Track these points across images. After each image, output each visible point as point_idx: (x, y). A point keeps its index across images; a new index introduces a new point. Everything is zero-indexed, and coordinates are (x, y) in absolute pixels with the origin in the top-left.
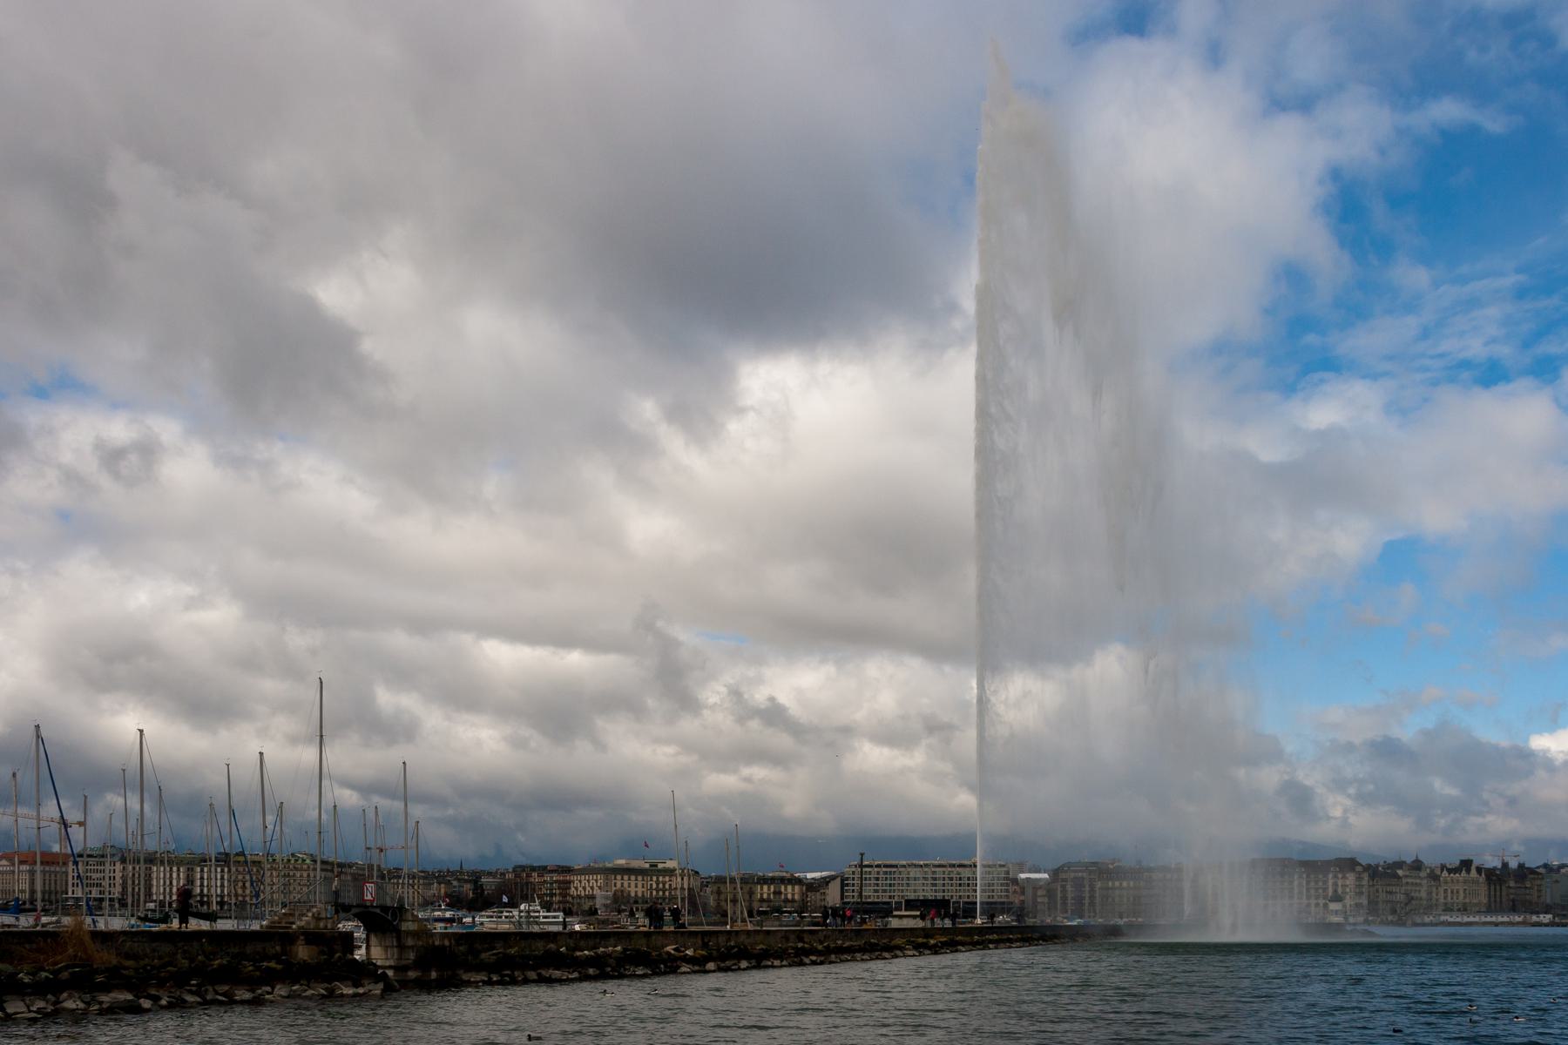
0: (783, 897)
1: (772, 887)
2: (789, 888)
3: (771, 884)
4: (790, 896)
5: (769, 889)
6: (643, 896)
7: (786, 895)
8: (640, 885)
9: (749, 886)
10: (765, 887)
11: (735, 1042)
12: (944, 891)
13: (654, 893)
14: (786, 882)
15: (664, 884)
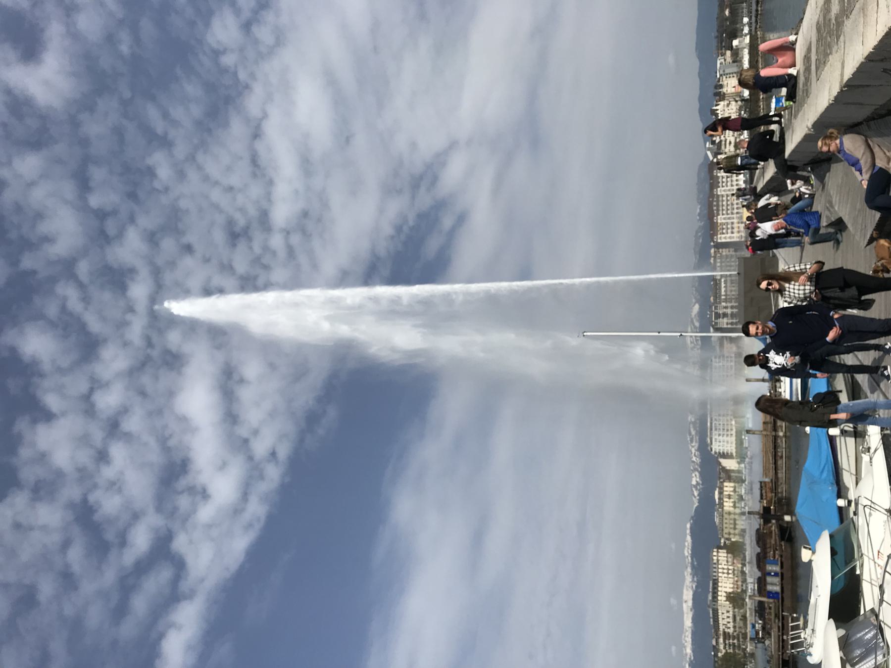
0: (732, 493)
1: (725, 500)
2: (725, 489)
4: (732, 489)
6: (733, 583)
7: (731, 491)
9: (724, 515)
10: (725, 504)
13: (731, 576)
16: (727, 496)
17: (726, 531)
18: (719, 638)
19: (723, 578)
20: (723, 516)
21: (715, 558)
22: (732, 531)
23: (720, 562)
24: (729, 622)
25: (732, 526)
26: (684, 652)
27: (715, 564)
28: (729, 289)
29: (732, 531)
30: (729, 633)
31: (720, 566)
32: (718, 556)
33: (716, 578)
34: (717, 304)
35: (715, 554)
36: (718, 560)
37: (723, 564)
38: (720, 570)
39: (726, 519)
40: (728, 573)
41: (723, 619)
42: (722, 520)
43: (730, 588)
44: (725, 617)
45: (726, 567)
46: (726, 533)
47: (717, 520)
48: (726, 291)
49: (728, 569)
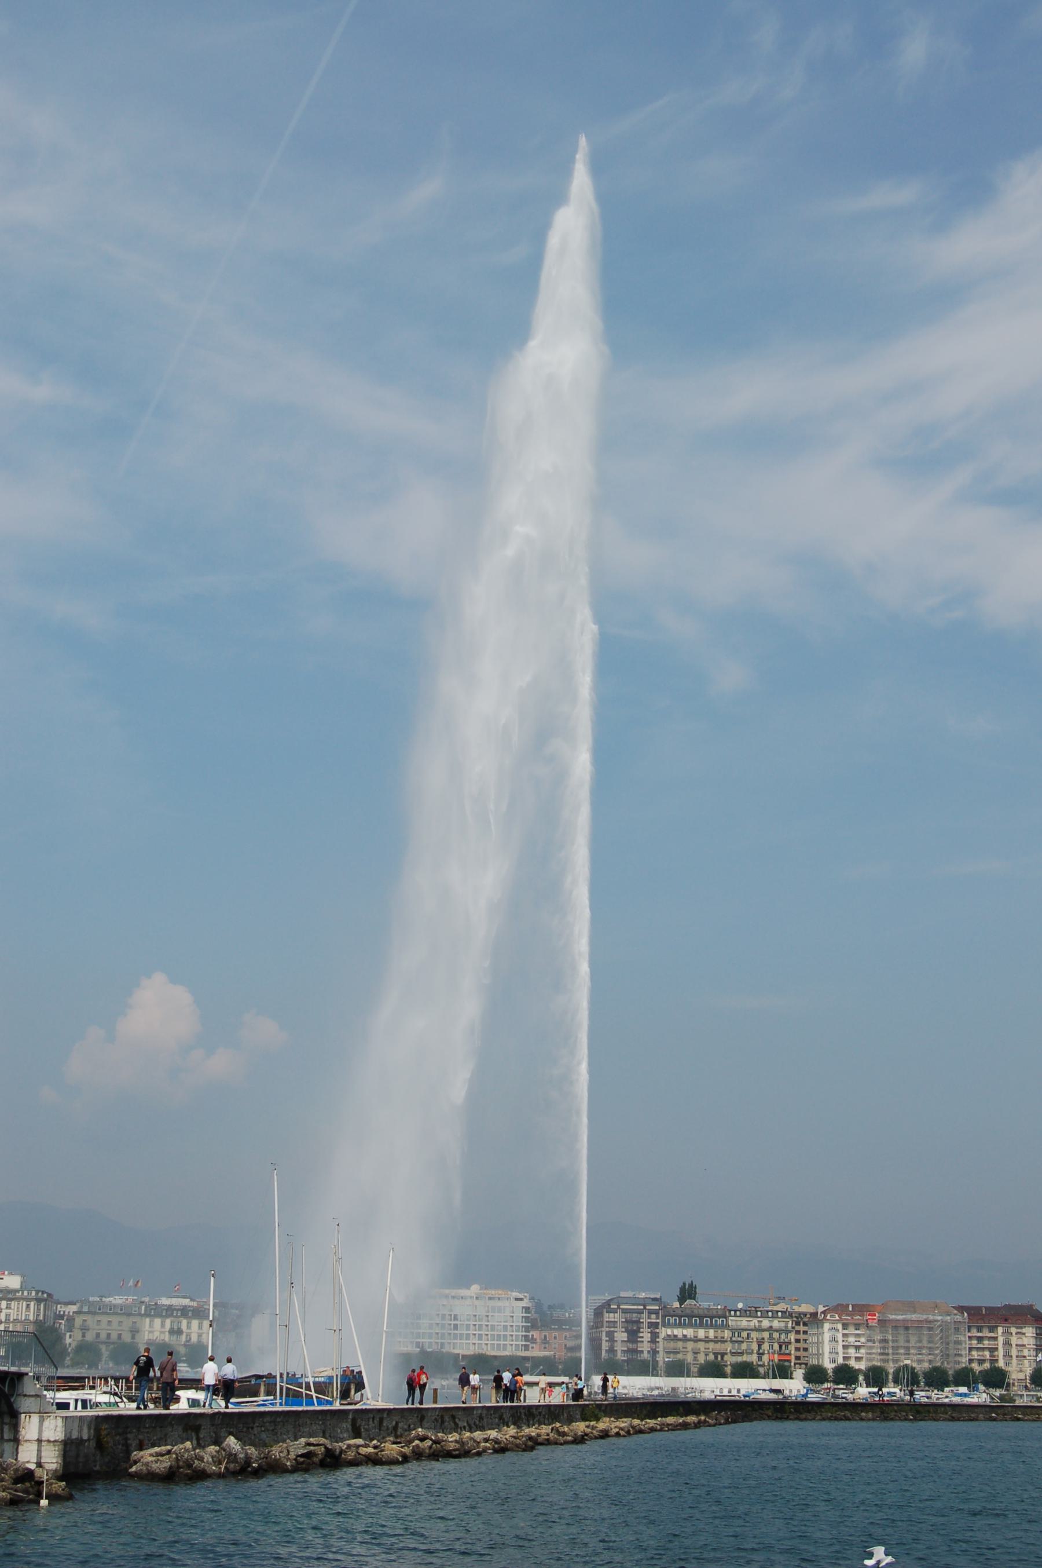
0: (184, 1338)
1: (168, 1322)
2: (195, 1323)
3: (167, 1316)
5: (163, 1325)
7: (188, 1335)
10: (158, 1321)
11: (969, 1458)
12: (480, 1337)
14: (190, 1314)
16: (176, 1327)
28: (701, 1346)
34: (664, 1316)
42: (116, 1314)
48: (696, 1340)
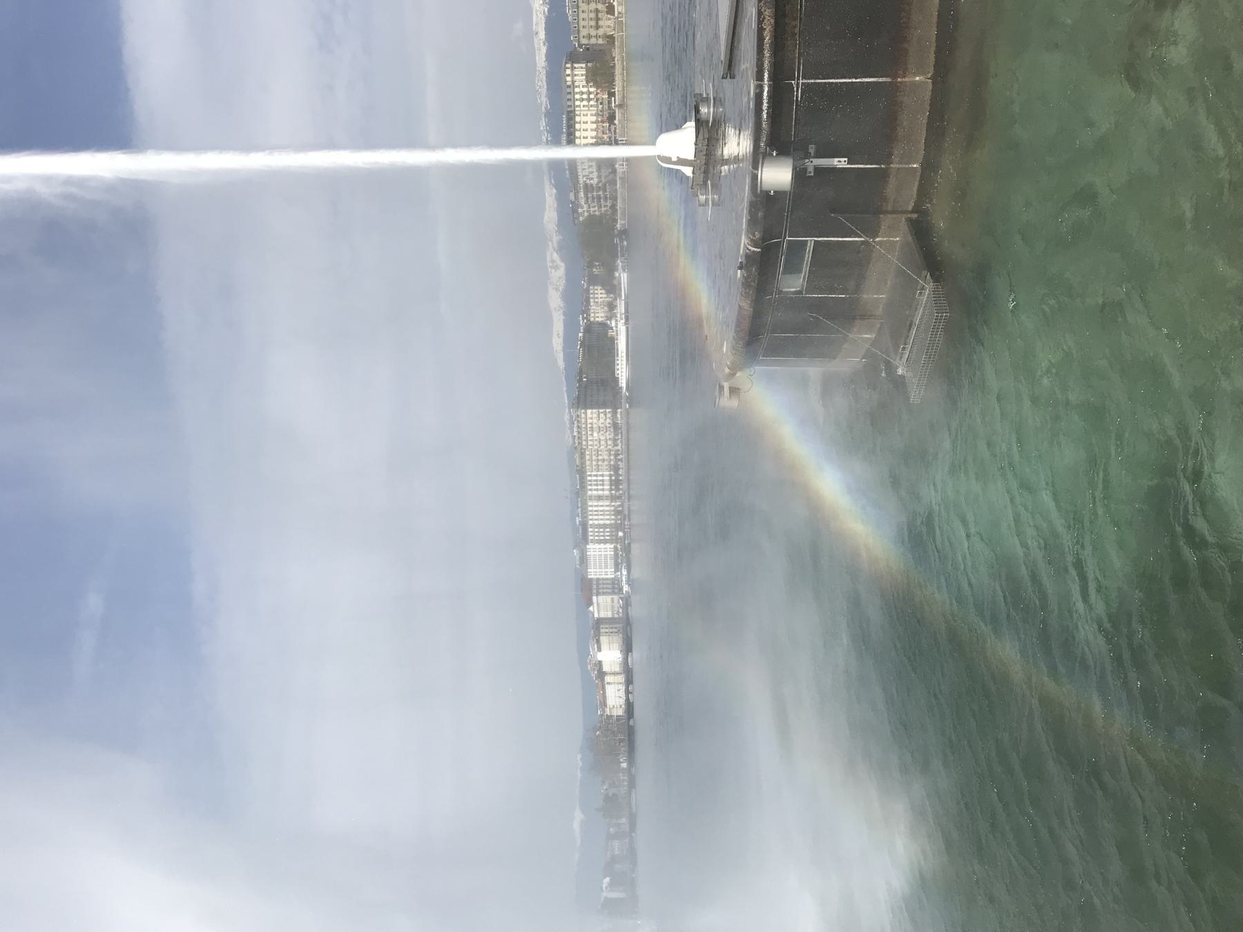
8: (584, 119)
13: (592, 103)
15: (582, 93)
17: (584, 32)
18: (578, 192)
19: (582, 108)
20: (578, 7)
21: (569, 79)
22: (593, 32)
23: (576, 84)
24: (592, 172)
25: (593, 23)
26: (539, 101)
27: (569, 87)
29: (593, 32)
30: (592, 185)
31: (577, 90)
32: (574, 75)
33: (572, 109)
35: (568, 72)
36: (573, 82)
37: (581, 86)
38: (577, 96)
39: (583, 12)
40: (589, 100)
41: (584, 169)
43: (592, 123)
44: (587, 167)
45: (585, 90)
46: (584, 37)
47: (569, 12)
49: (590, 93)
